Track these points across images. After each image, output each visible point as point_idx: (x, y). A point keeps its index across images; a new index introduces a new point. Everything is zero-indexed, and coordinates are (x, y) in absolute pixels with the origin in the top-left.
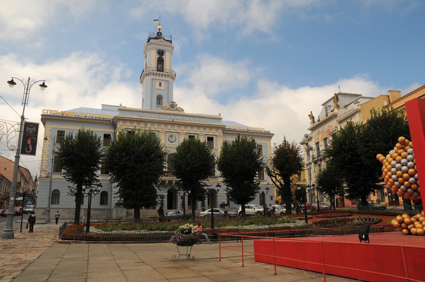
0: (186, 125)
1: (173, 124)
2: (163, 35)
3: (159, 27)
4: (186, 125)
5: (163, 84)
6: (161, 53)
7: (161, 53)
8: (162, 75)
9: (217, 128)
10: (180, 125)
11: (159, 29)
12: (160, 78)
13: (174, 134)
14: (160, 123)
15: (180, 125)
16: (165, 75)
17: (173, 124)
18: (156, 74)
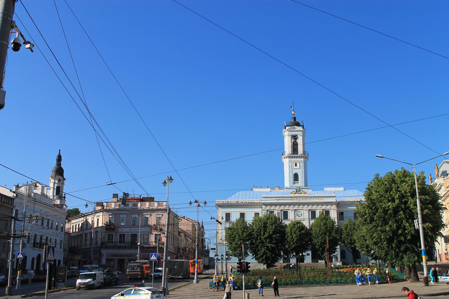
0: (308, 204)
1: (299, 204)
2: (297, 120)
3: (293, 113)
4: (308, 204)
5: (298, 164)
6: (295, 137)
7: (295, 137)
8: (297, 156)
9: (331, 203)
10: (304, 204)
11: (294, 114)
12: (296, 159)
13: (300, 211)
14: (290, 204)
15: (304, 204)
16: (299, 156)
17: (299, 204)
18: (292, 157)
